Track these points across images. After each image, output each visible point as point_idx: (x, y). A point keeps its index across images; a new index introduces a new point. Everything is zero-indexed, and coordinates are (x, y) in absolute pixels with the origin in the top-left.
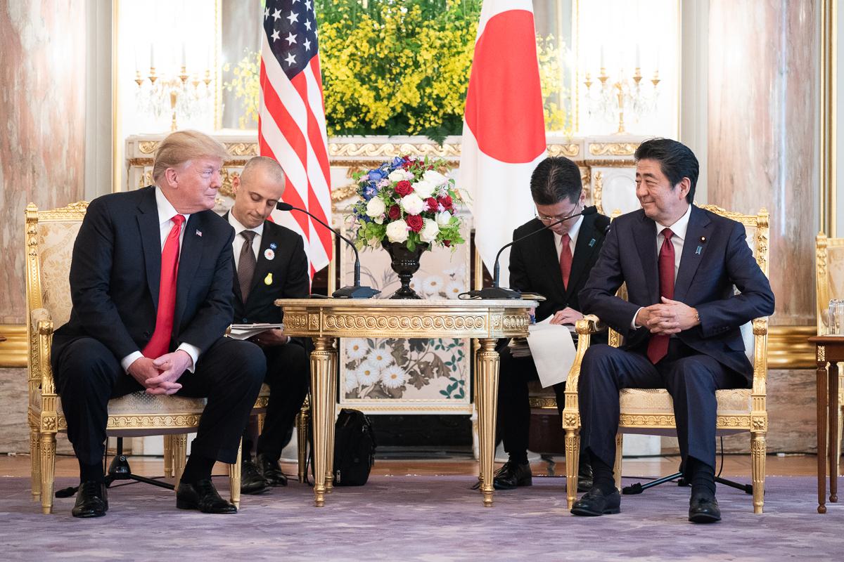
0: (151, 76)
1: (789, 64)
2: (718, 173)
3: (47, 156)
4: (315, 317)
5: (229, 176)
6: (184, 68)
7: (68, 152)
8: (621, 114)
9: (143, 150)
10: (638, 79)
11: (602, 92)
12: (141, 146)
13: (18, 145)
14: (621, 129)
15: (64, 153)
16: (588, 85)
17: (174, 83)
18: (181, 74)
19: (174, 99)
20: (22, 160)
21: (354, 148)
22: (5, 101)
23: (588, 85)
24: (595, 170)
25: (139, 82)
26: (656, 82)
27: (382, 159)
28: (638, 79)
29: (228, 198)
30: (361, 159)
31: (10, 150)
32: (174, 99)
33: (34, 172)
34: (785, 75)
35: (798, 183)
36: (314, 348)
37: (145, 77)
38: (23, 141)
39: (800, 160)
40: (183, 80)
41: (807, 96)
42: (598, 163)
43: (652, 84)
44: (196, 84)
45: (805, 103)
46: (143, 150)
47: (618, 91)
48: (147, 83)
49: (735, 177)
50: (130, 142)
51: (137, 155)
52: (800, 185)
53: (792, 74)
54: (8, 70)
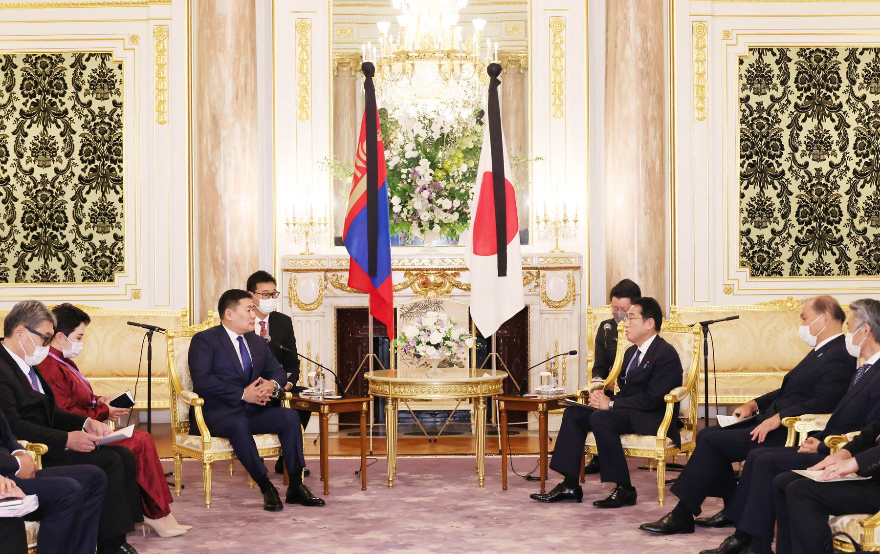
0: (293, 222)
1: (650, 210)
2: (611, 269)
3: (237, 265)
4: (387, 386)
5: (339, 278)
6: (312, 217)
7: (249, 262)
8: (557, 241)
9: (291, 264)
10: (565, 221)
11: (545, 228)
12: (290, 261)
13: (222, 258)
14: (557, 247)
15: (247, 263)
16: (538, 223)
17: (306, 225)
18: (310, 221)
19: (307, 233)
20: (225, 267)
21: (407, 261)
22: (214, 234)
23: (538, 223)
24: (542, 272)
25: (288, 225)
26: (576, 221)
27: (422, 267)
28: (565, 221)
29: (338, 289)
30: (411, 267)
31: (217, 262)
32: (307, 233)
33: (230, 274)
34: (648, 215)
35: (656, 274)
36: (387, 403)
37: (291, 221)
38: (224, 256)
39: (657, 262)
40: (311, 224)
41: (661, 226)
42: (543, 269)
43: (574, 223)
44: (320, 224)
45: (659, 230)
46: (291, 264)
47: (555, 226)
48: (291, 226)
49: (621, 272)
50: (283, 260)
51: (287, 268)
52: (657, 276)
53: (652, 214)
54: (216, 218)
